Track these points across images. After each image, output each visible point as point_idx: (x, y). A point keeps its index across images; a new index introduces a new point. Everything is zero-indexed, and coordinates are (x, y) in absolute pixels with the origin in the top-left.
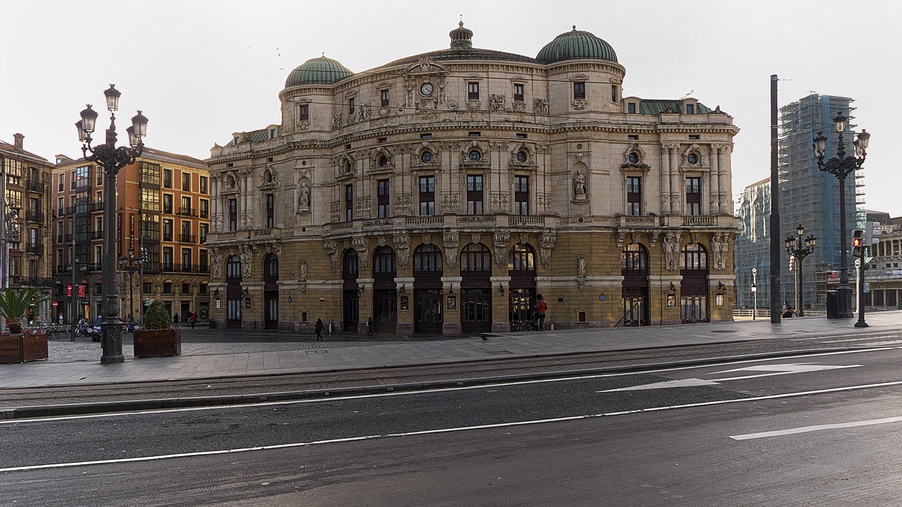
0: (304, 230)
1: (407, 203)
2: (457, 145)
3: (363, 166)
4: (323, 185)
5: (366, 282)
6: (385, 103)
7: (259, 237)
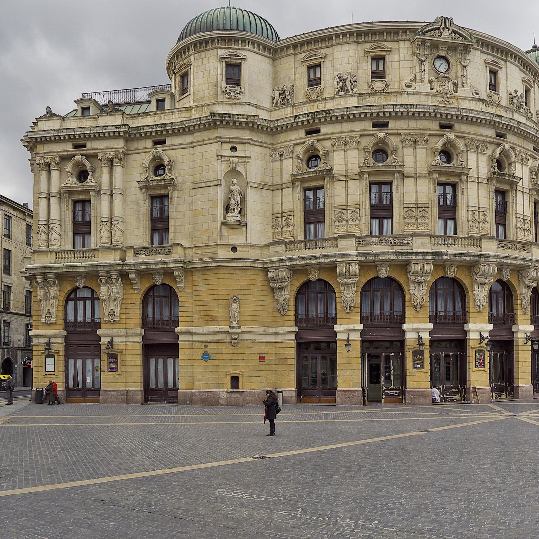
0: (234, 249)
1: (424, 217)
2: (486, 144)
3: (346, 160)
4: (262, 186)
5: (349, 329)
6: (378, 75)
7: (142, 258)
